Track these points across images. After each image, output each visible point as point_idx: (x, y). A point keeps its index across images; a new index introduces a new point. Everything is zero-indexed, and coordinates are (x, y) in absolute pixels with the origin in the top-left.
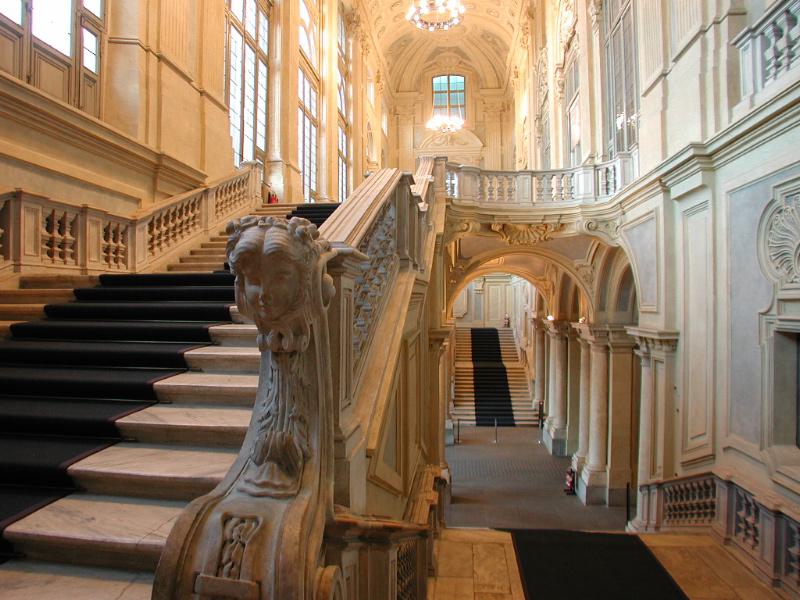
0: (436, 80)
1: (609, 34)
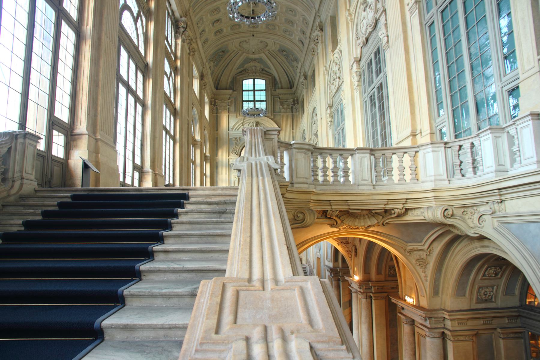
0: (245, 82)
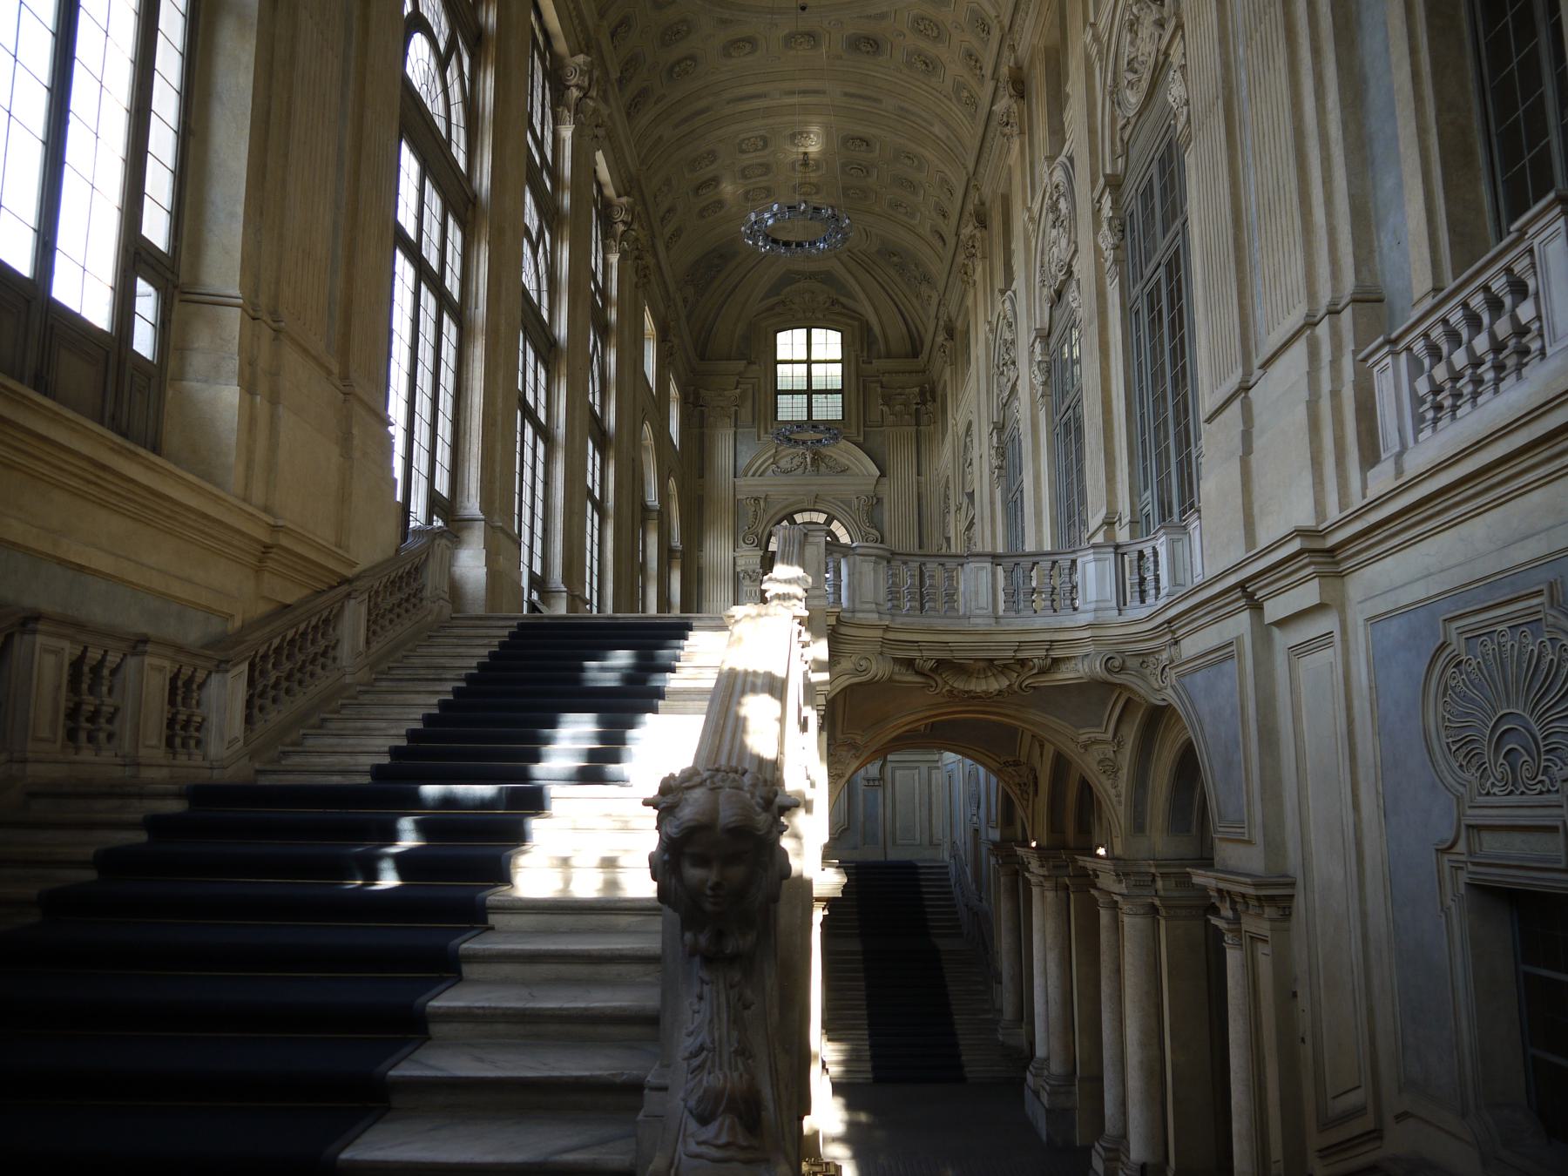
0: (783, 338)
1: (1139, 286)
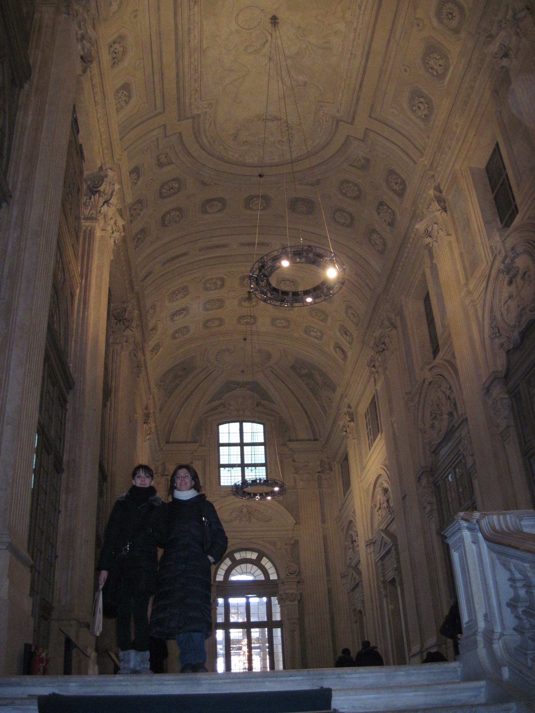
0: (223, 428)
